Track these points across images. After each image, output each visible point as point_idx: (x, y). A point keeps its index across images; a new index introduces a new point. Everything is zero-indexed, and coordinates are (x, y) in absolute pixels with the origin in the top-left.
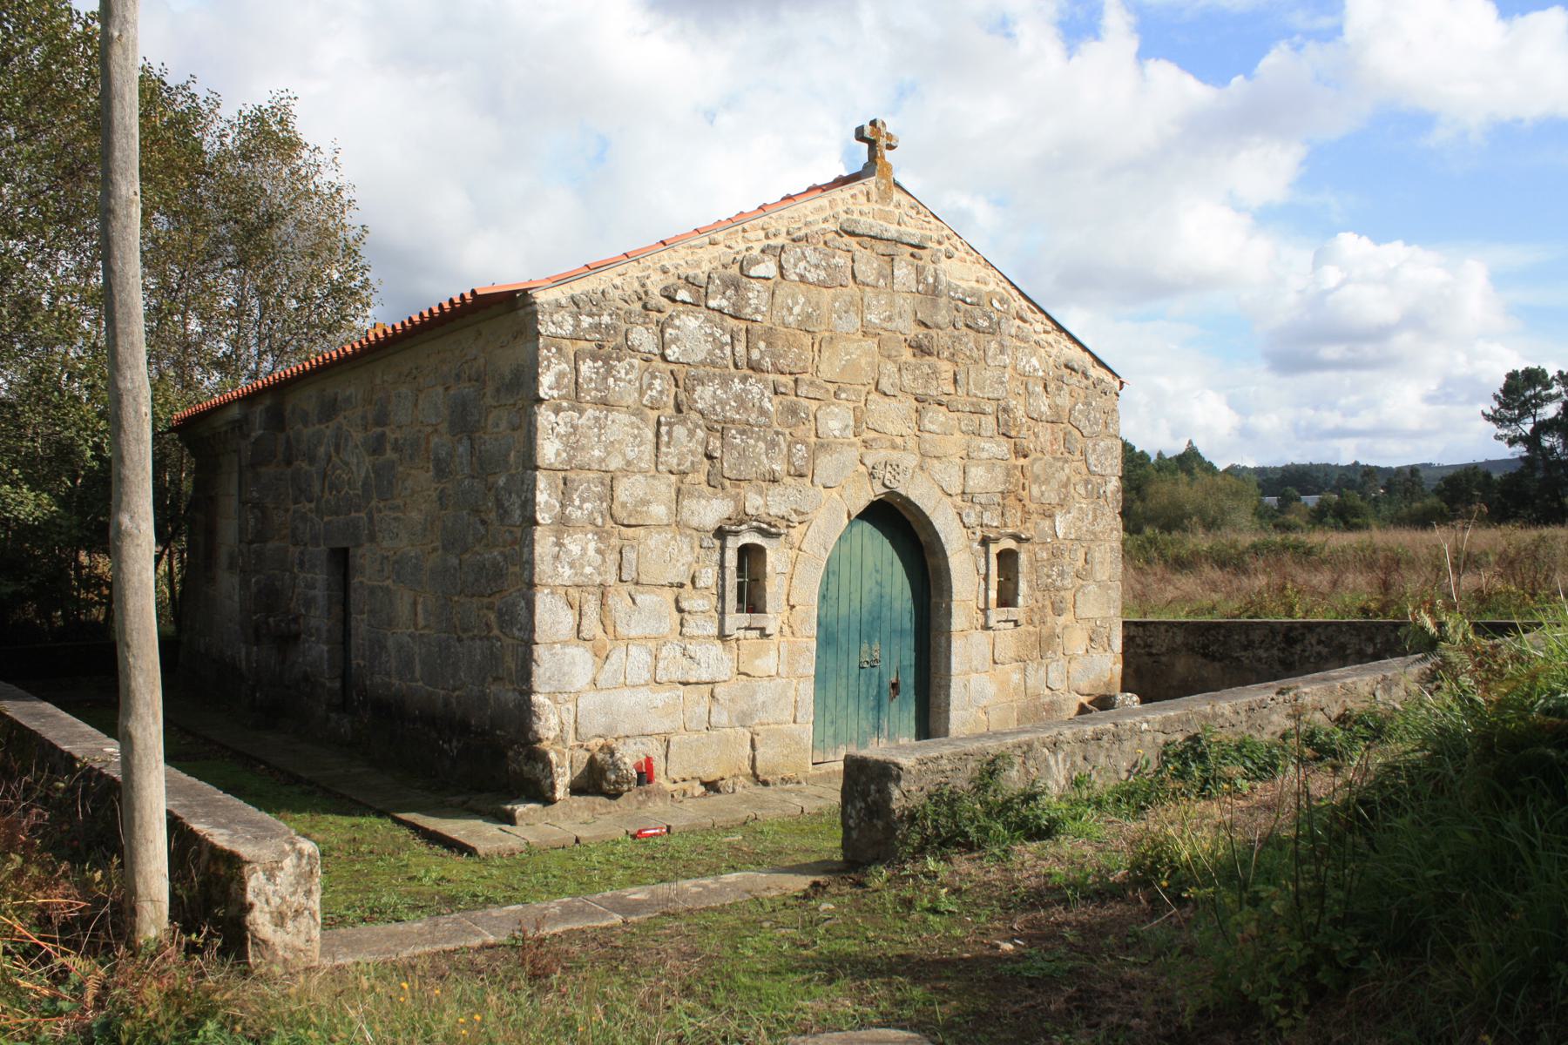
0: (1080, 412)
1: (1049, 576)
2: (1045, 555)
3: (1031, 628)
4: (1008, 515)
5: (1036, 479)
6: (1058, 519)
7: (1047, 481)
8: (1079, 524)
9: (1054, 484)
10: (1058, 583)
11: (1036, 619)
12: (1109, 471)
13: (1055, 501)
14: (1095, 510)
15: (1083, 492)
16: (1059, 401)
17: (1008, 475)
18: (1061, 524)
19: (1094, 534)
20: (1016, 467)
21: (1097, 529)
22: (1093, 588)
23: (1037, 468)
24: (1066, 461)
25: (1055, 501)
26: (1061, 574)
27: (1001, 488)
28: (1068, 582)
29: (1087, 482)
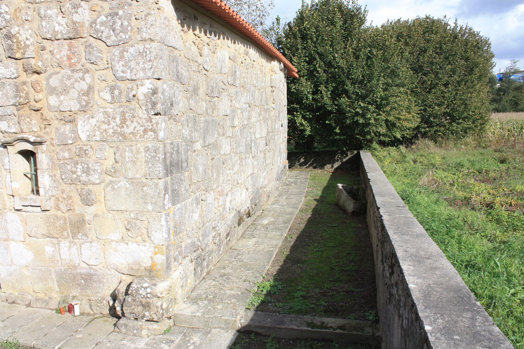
0: (102, 24)
1: (74, 173)
2: (66, 155)
3: (59, 214)
4: (22, 122)
5: (53, 91)
6: (80, 124)
7: (65, 91)
8: (104, 127)
9: (74, 93)
10: (84, 178)
11: (62, 206)
12: (141, 74)
13: (75, 107)
14: (123, 114)
15: (108, 97)
16: (76, 18)
17: (17, 90)
18: (84, 128)
19: (123, 135)
20: (25, 83)
21: (127, 131)
22: (123, 183)
23: (54, 82)
24: (87, 71)
25: (75, 107)
26: (87, 171)
27: (12, 101)
28: (95, 178)
29: (112, 89)
